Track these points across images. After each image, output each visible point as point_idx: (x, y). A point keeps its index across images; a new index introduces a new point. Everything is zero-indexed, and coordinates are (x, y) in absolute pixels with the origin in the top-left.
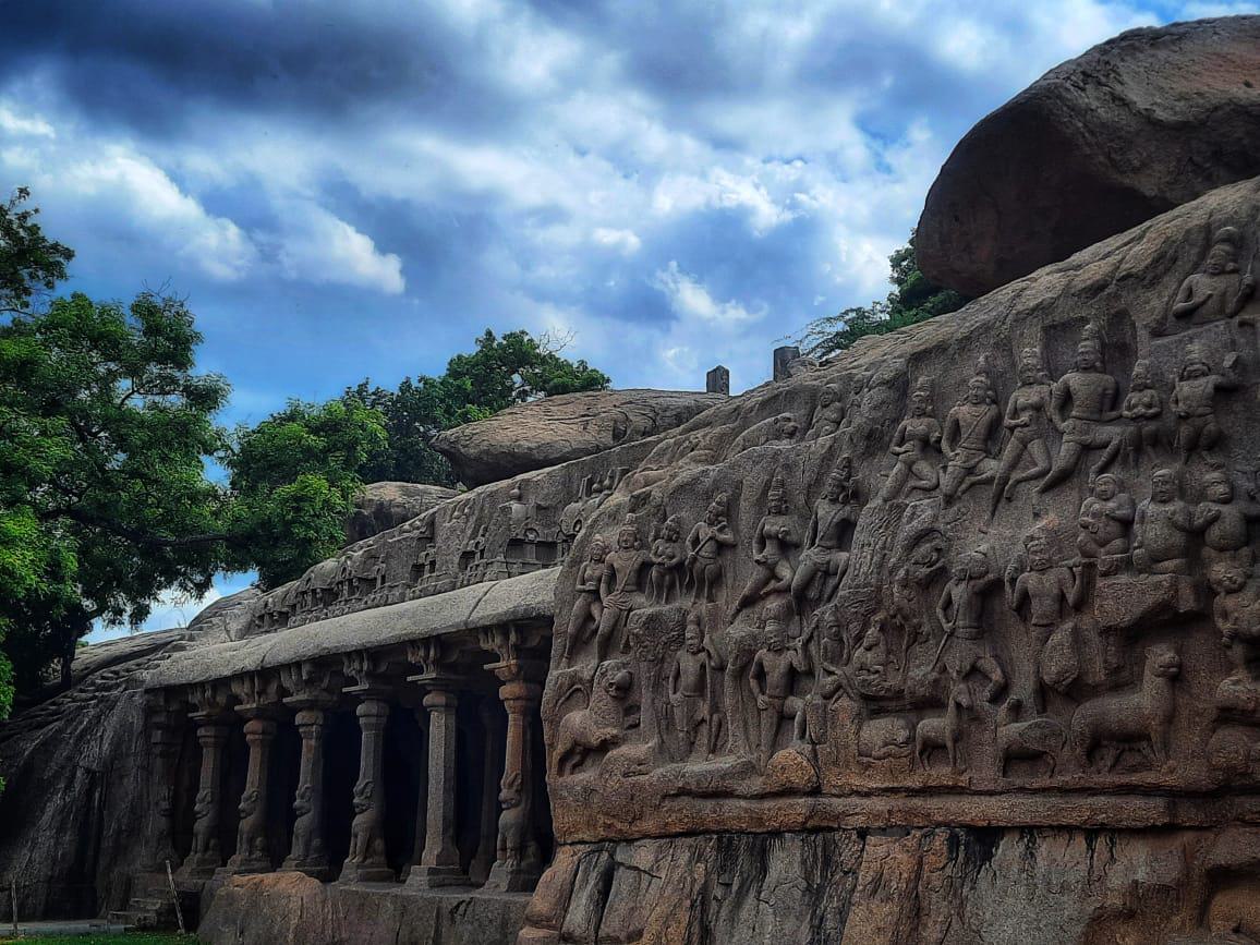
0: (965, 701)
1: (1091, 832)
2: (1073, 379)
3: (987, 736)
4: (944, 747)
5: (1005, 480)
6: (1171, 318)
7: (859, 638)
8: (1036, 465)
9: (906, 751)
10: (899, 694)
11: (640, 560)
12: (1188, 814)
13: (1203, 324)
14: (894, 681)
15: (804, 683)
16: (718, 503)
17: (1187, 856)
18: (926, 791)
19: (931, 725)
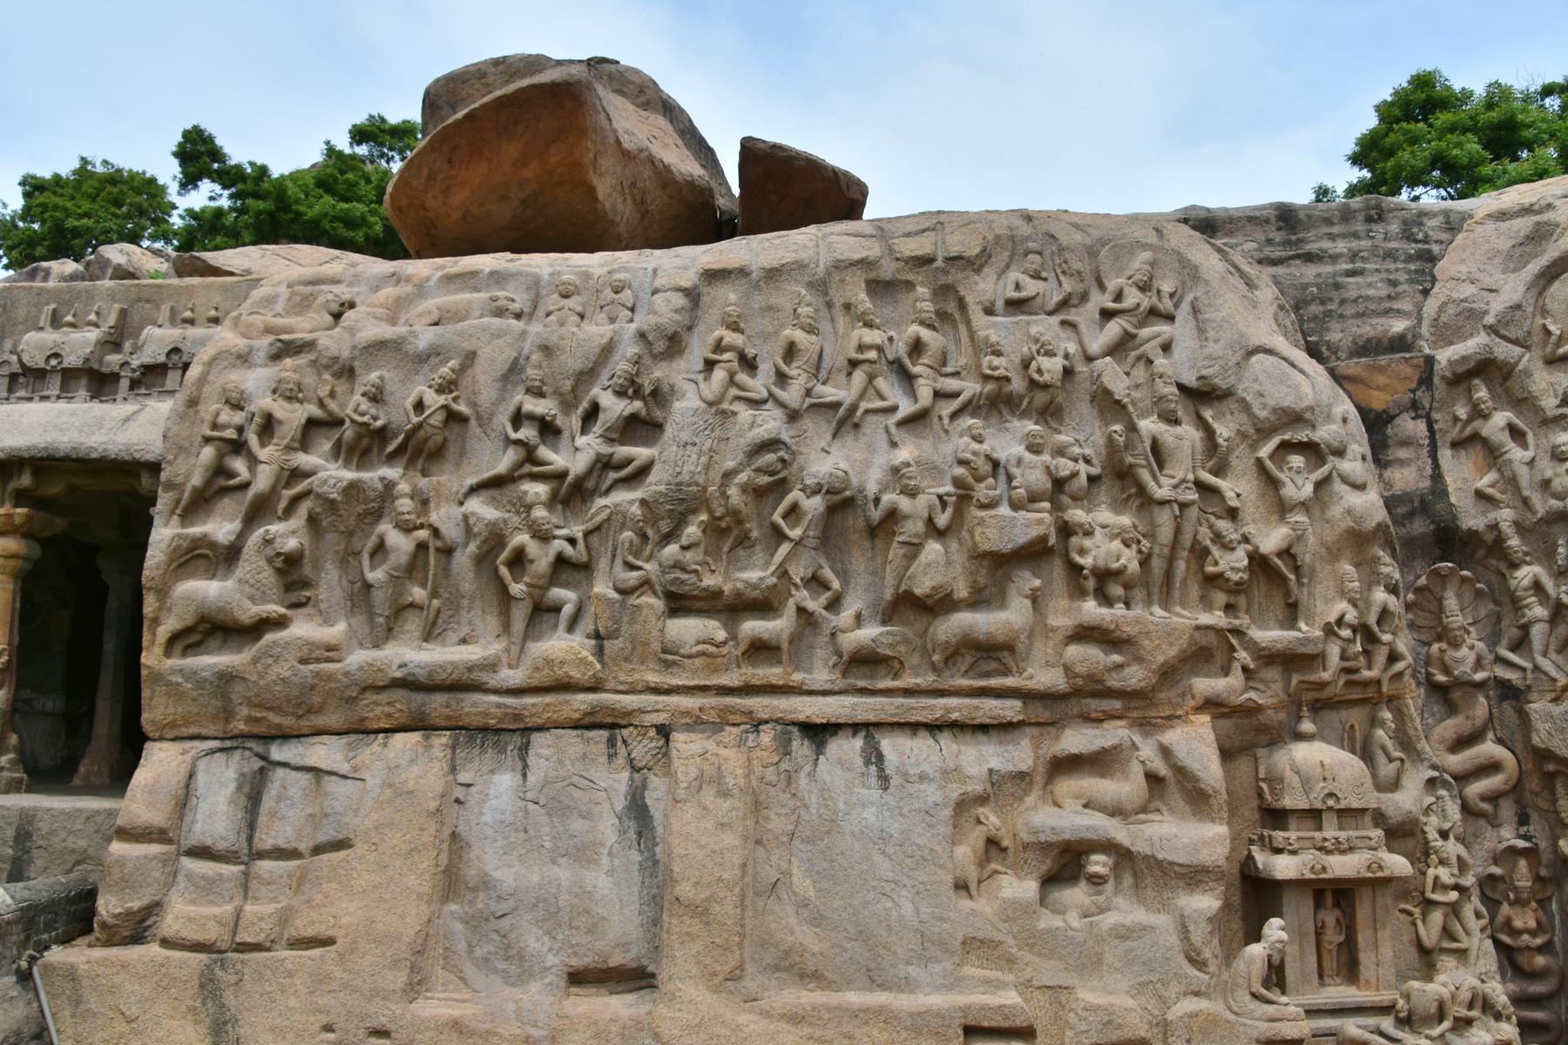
0: (811, 605)
1: (933, 728)
2: (925, 334)
3: (823, 639)
4: (778, 648)
5: (854, 408)
6: (1000, 304)
7: (668, 538)
8: (883, 398)
9: (724, 650)
10: (716, 594)
11: (305, 416)
13: (1030, 314)
14: (709, 581)
15: (566, 575)
16: (453, 370)
17: (1036, 747)
18: (748, 690)
19: (753, 627)
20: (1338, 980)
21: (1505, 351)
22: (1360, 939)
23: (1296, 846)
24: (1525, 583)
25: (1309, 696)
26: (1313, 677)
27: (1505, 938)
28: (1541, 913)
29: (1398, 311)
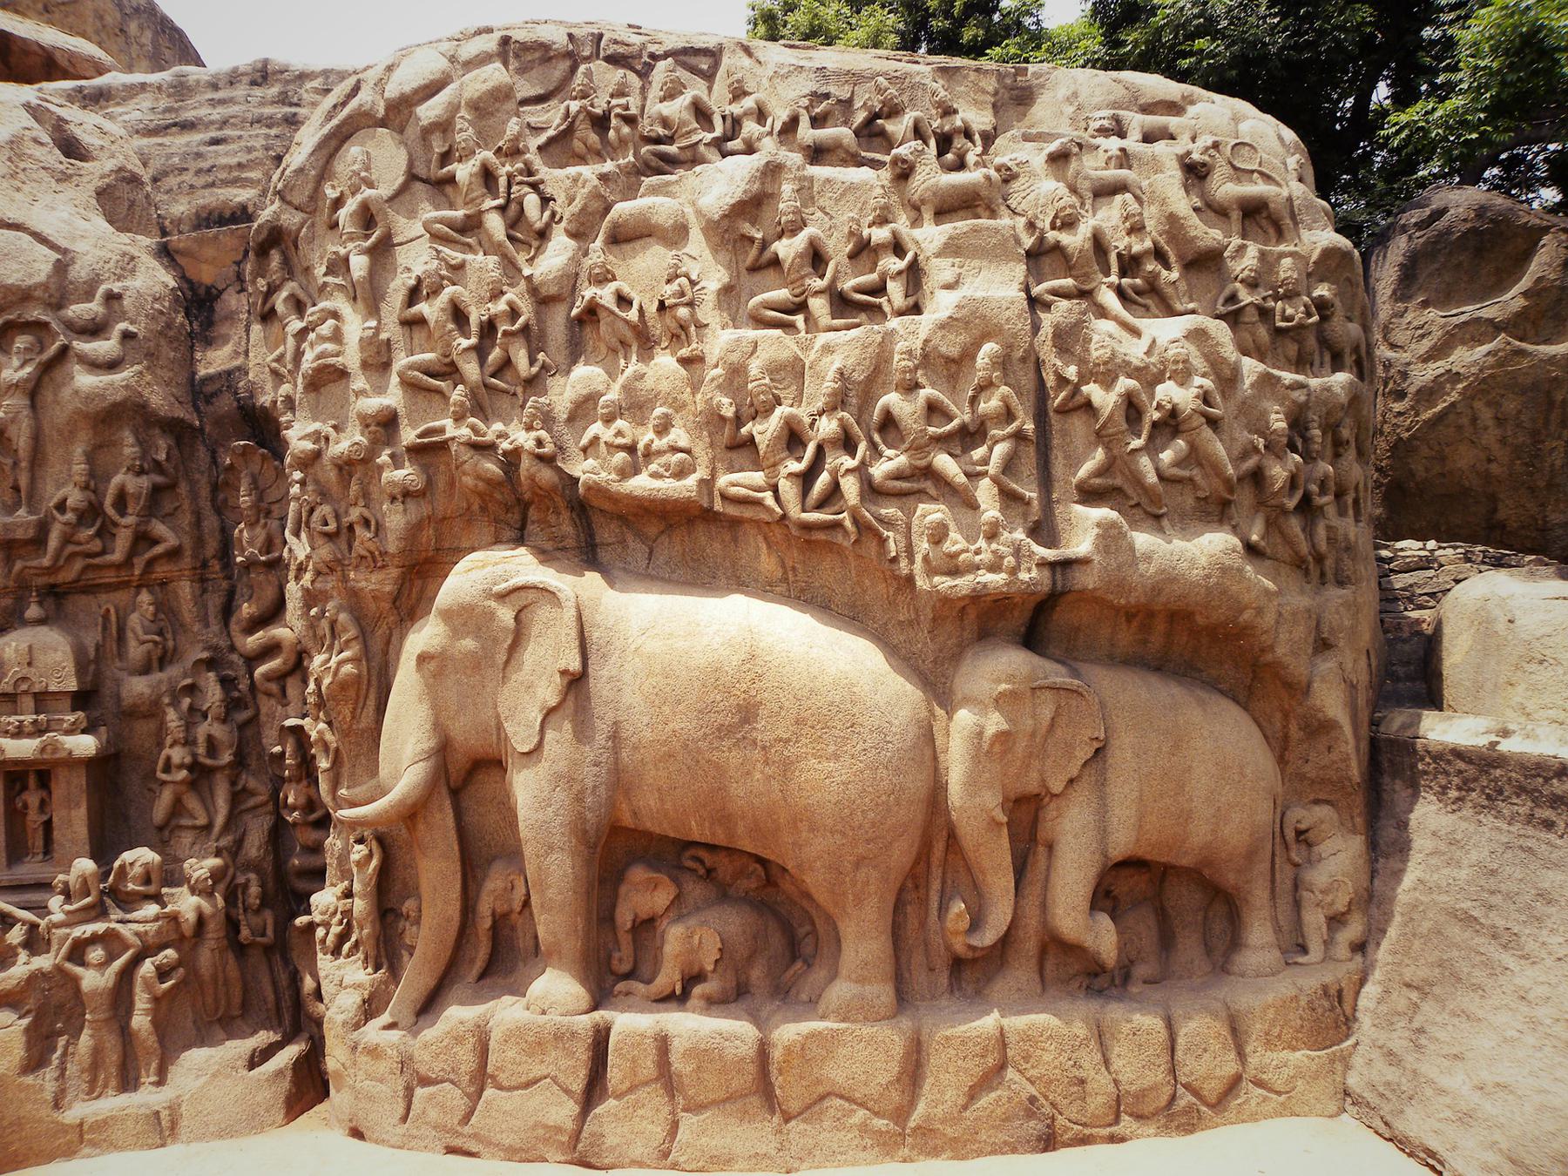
20: (40, 857)
21: (291, 219)
22: (55, 819)
26: (35, 563)
29: (246, 179)
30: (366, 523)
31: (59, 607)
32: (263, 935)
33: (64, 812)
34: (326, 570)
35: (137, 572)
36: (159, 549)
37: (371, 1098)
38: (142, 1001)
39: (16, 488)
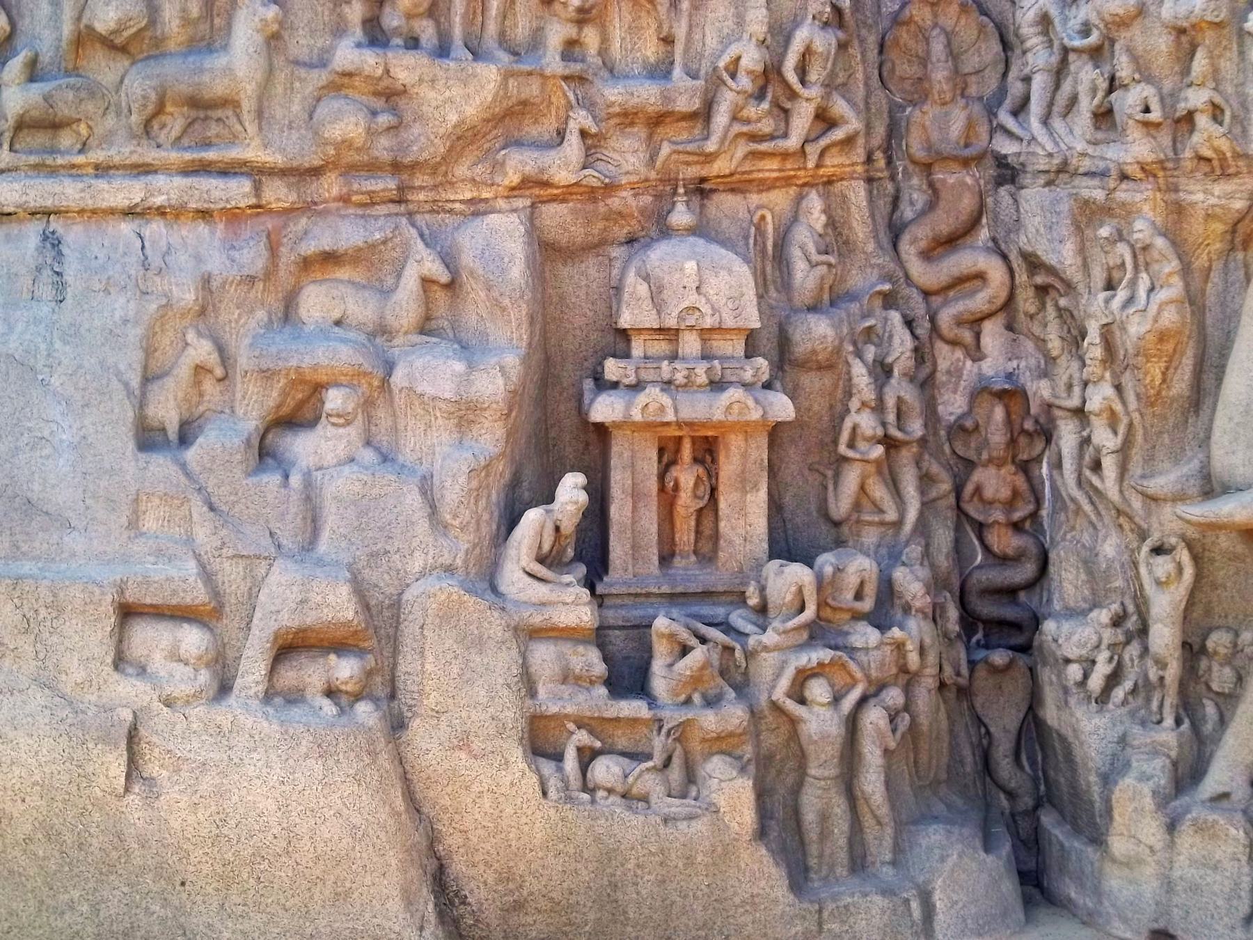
12: (278, 194)
22: (722, 505)
23: (632, 379)
24: (1031, 15)
25: (693, 172)
27: (972, 509)
28: (1020, 482)
30: (1216, 112)
31: (702, 206)
32: (958, 674)
33: (735, 496)
34: (1140, 175)
35: (811, 165)
36: (838, 134)
37: (1195, 888)
38: (872, 755)
39: (668, 41)
